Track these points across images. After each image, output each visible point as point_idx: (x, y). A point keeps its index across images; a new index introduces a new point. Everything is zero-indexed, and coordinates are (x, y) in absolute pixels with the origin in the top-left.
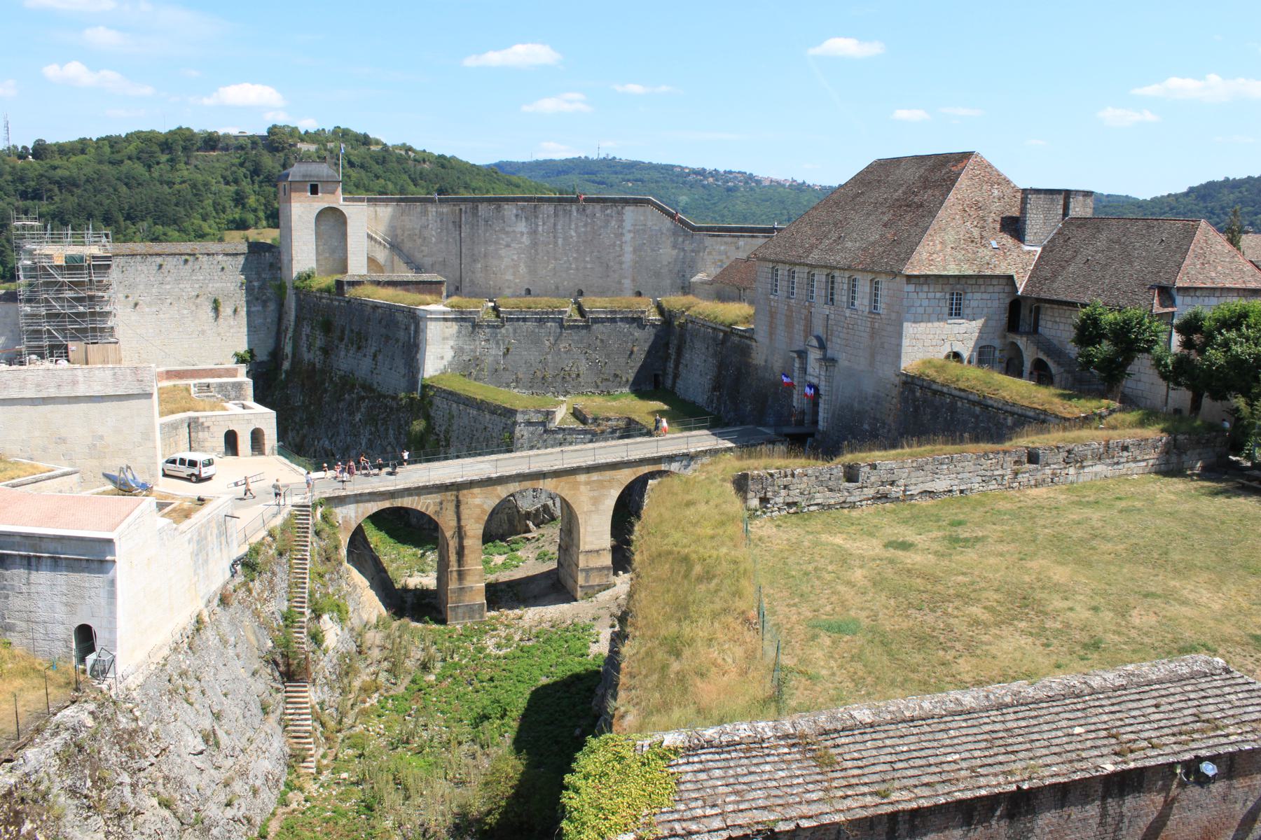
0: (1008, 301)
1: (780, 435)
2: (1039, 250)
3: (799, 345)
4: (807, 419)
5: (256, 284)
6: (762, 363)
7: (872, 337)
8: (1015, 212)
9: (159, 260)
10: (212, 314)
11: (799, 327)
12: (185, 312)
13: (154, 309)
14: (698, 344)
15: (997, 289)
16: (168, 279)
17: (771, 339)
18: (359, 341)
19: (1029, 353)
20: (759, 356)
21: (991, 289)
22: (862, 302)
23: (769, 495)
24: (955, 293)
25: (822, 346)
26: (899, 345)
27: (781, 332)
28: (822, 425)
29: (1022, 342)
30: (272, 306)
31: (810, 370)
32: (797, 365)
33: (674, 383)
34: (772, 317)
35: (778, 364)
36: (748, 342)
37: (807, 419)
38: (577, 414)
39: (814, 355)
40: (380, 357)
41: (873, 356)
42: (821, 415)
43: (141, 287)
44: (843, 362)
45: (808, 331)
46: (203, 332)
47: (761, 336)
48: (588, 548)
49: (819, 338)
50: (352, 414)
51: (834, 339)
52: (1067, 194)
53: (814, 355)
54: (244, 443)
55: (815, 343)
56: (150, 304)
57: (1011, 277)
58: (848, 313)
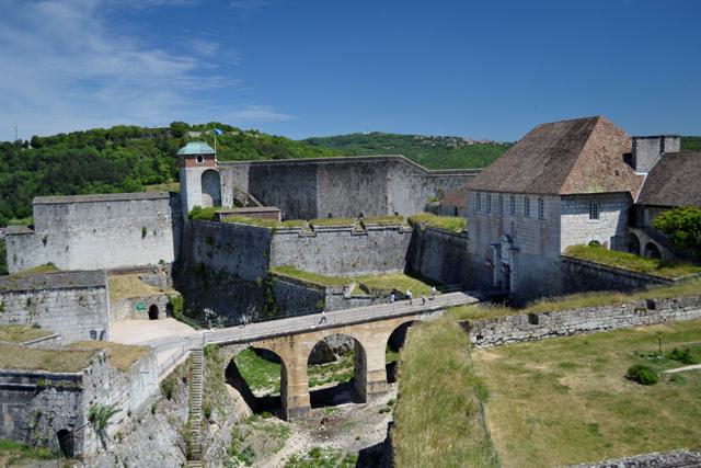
0: (627, 207)
2: (646, 174)
4: (503, 286)
7: (541, 234)
8: (629, 151)
9: (108, 204)
10: (141, 234)
11: (495, 230)
13: (105, 234)
14: (435, 244)
15: (620, 200)
18: (229, 248)
19: (643, 240)
20: (472, 248)
21: (616, 201)
22: (534, 213)
23: (483, 334)
24: (592, 204)
25: (510, 241)
26: (559, 238)
27: (484, 233)
28: (512, 289)
29: (638, 233)
31: (503, 256)
35: (483, 253)
36: (463, 240)
37: (503, 286)
38: (363, 288)
39: (505, 246)
40: (242, 258)
41: (542, 246)
42: (512, 283)
44: (524, 250)
45: (501, 232)
47: (472, 236)
49: (508, 236)
50: (226, 291)
51: (518, 237)
52: (663, 138)
53: (505, 246)
55: (506, 239)
56: (103, 230)
57: (628, 193)
58: (525, 219)
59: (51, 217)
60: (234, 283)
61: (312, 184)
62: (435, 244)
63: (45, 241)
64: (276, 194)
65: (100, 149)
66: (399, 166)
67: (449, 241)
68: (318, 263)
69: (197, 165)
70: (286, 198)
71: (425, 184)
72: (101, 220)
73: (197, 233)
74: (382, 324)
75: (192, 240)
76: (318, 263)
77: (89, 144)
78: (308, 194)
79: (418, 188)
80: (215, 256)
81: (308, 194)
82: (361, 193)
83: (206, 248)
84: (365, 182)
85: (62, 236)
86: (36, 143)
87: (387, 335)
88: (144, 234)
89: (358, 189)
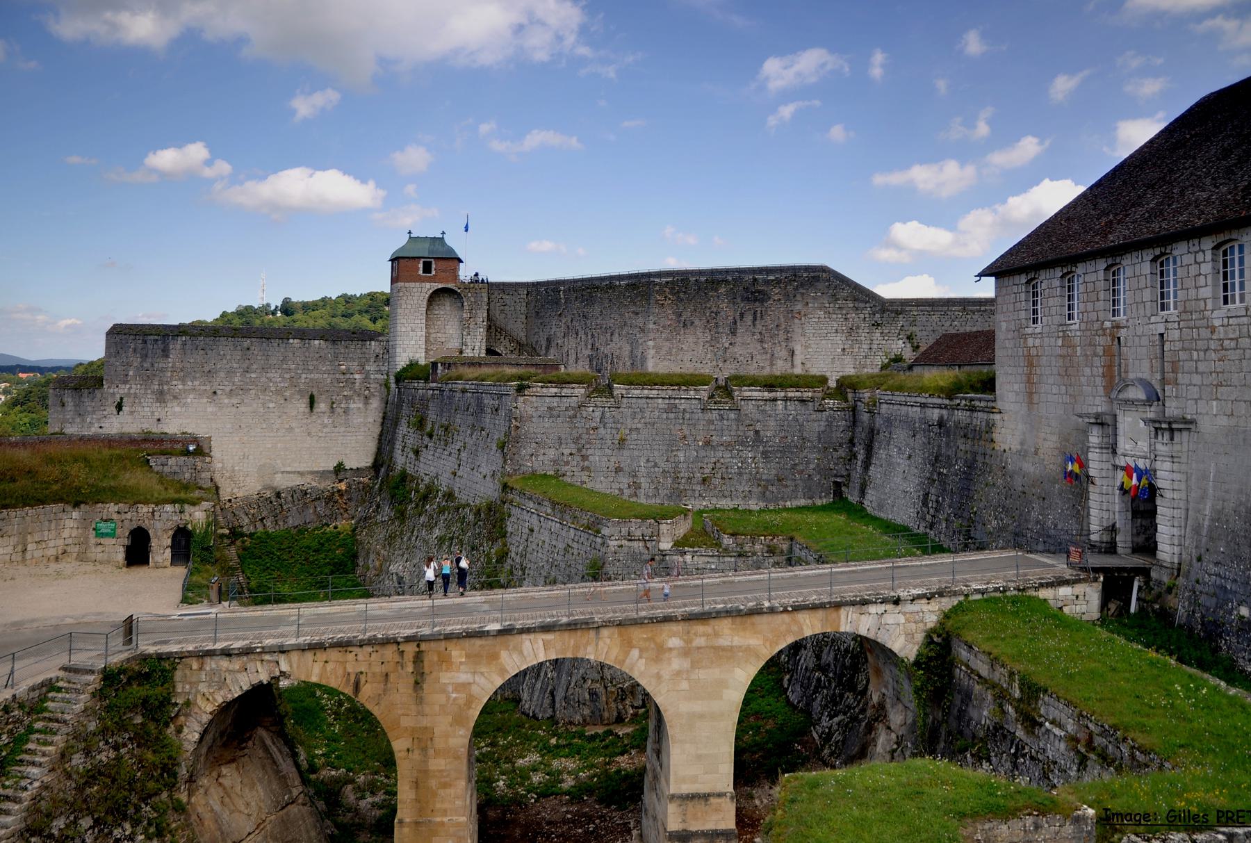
1: (1084, 569)
3: (1099, 405)
5: (357, 376)
6: (1016, 446)
11: (1091, 374)
12: (271, 405)
13: (235, 401)
14: (900, 435)
16: (255, 366)
17: (1031, 403)
28: (1168, 548)
30: (375, 403)
31: (1124, 445)
32: (1095, 438)
33: (863, 492)
34: (1031, 365)
37: (1123, 541)
40: (463, 454)
43: (222, 374)
46: (291, 429)
48: (686, 789)
54: (161, 549)
59: (136, 361)
60: (442, 511)
61: (640, 320)
62: (900, 435)
63: (119, 407)
64: (571, 343)
65: (374, 320)
66: (820, 285)
67: (941, 424)
68: (618, 470)
69: (422, 280)
70: (588, 352)
71: (876, 325)
72: (230, 373)
73: (405, 410)
74: (727, 634)
75: (396, 423)
76: (618, 470)
77: (360, 312)
78: (633, 343)
79: (863, 334)
80: (425, 454)
81: (633, 343)
82: (739, 340)
83: (413, 439)
84: (749, 319)
85: (150, 398)
86: (288, 308)
87: (743, 676)
88: (312, 402)
89: (734, 333)
